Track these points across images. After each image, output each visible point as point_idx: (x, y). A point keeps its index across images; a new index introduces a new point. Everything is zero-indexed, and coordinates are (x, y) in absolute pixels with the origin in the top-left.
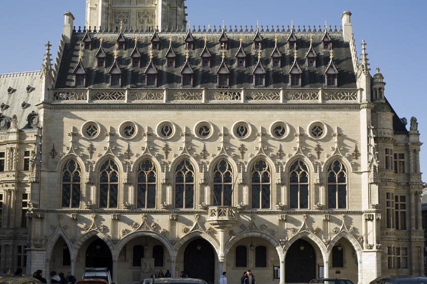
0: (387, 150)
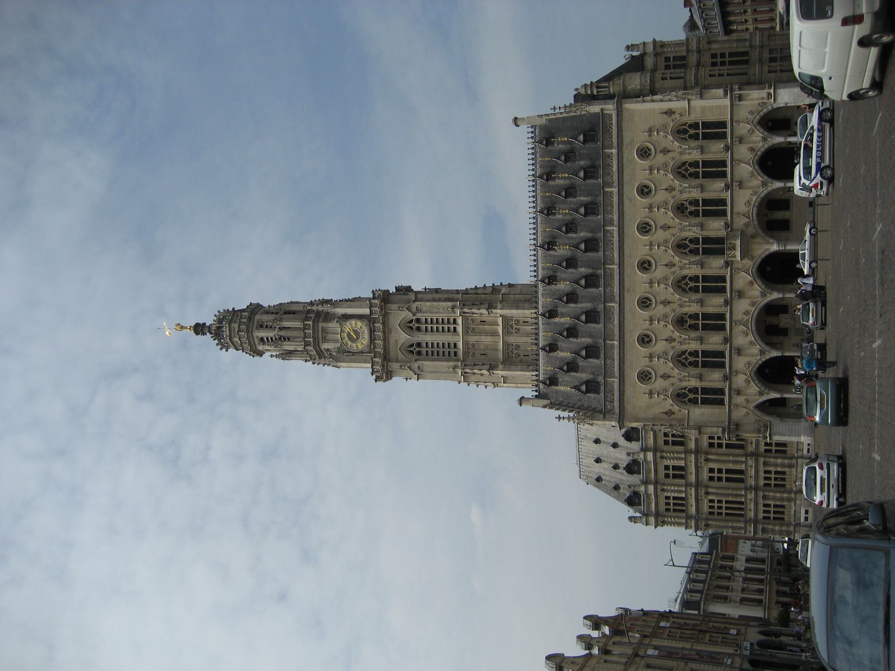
0: (663, 79)
